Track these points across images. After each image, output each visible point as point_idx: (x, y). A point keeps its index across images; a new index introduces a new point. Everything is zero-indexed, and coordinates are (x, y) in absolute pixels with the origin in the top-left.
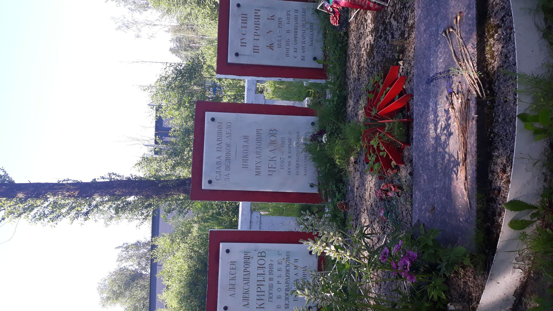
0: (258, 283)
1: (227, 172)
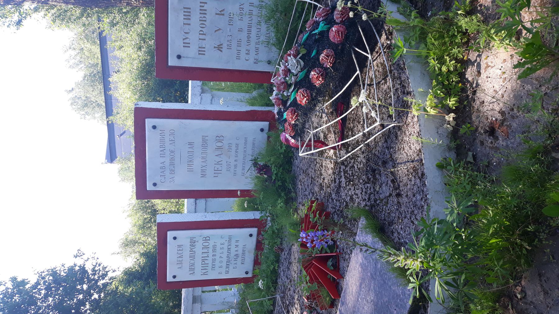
1: (172, 176)
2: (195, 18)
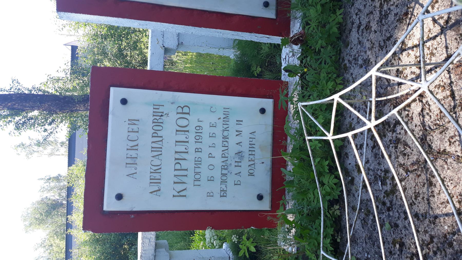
0: (177, 156)
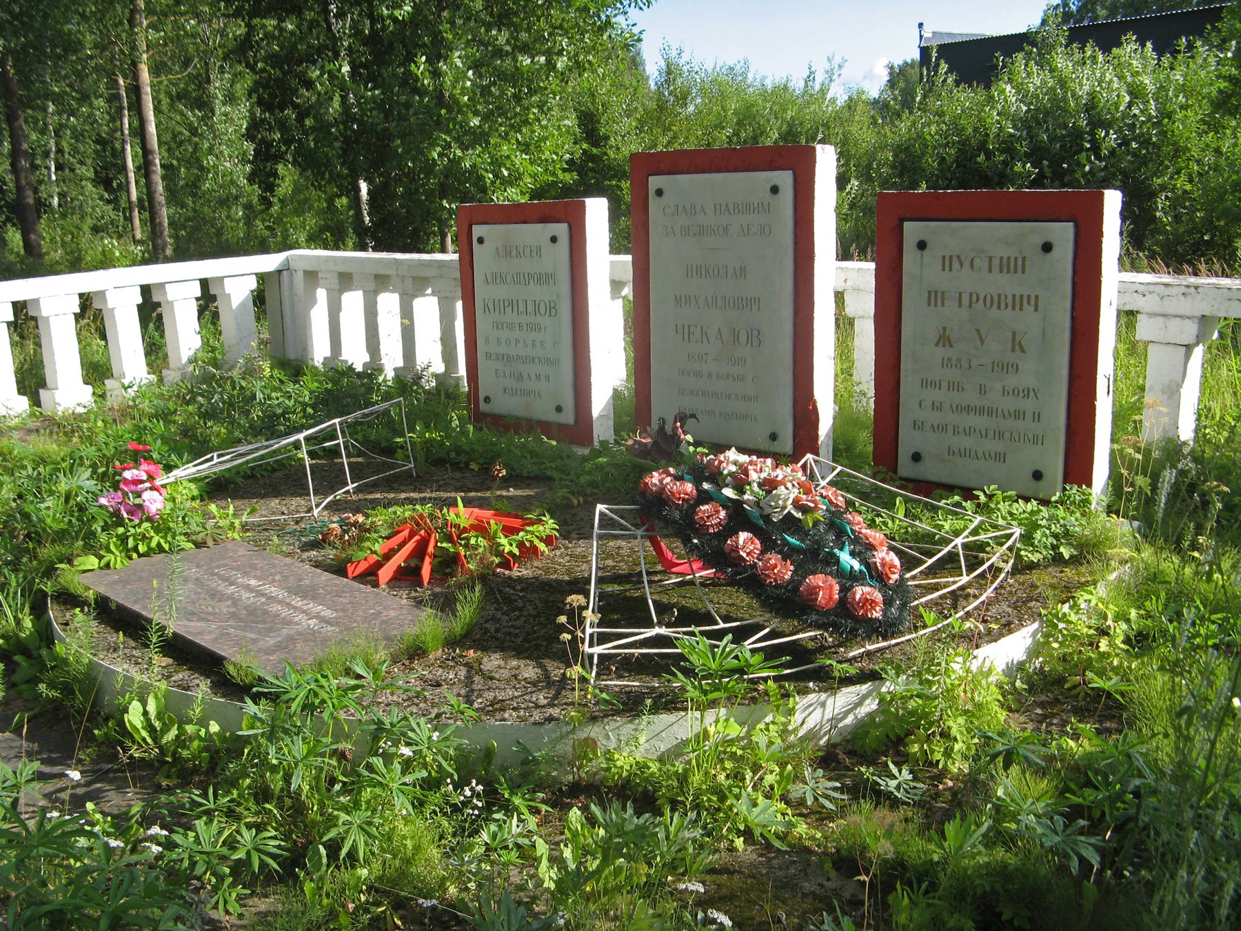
2: (1007, 285)
